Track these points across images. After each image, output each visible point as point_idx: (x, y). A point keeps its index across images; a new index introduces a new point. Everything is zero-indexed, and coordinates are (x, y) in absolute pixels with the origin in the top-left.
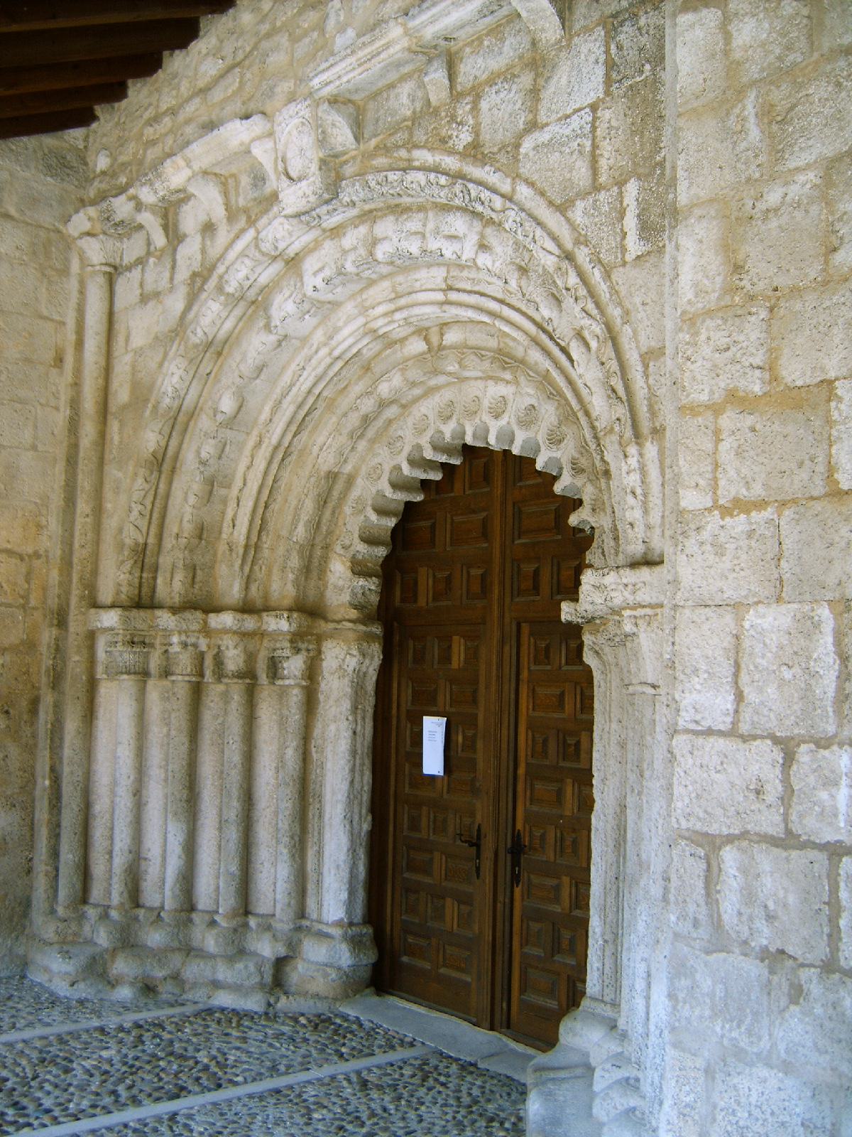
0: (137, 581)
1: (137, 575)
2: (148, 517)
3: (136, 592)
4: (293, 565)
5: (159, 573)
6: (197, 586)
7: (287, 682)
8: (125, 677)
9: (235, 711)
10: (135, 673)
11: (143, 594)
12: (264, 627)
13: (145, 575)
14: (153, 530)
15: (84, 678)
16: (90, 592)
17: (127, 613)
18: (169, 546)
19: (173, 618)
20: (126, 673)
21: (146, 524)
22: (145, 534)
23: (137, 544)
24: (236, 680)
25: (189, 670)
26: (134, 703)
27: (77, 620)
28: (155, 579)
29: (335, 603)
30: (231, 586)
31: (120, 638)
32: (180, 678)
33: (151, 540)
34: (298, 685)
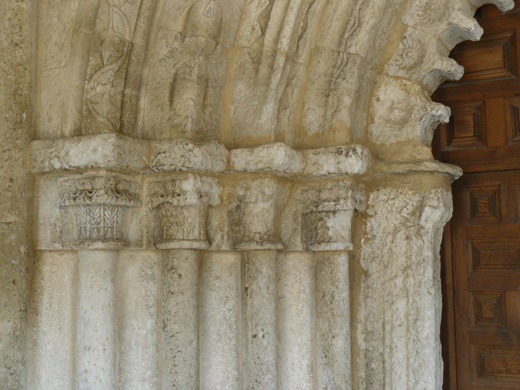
0: (119, 97)
1: (120, 89)
2: (139, 4)
3: (119, 114)
4: (348, 86)
5: (143, 90)
6: (208, 111)
7: (334, 246)
8: (99, 245)
9: (264, 291)
10: (112, 239)
11: (126, 119)
12: (311, 169)
13: (128, 91)
14: (142, 26)
15: (23, 249)
16: (29, 117)
17: (121, 142)
18: (165, 51)
19: (197, 150)
20: (98, 239)
21: (136, 13)
22: (133, 28)
23: (123, 42)
24: (267, 246)
25: (196, 233)
26: (109, 286)
27: (10, 158)
28: (138, 98)
29: (393, 140)
30: (258, 113)
31: (99, 183)
32: (186, 244)
33: (139, 41)
34: (345, 250)
